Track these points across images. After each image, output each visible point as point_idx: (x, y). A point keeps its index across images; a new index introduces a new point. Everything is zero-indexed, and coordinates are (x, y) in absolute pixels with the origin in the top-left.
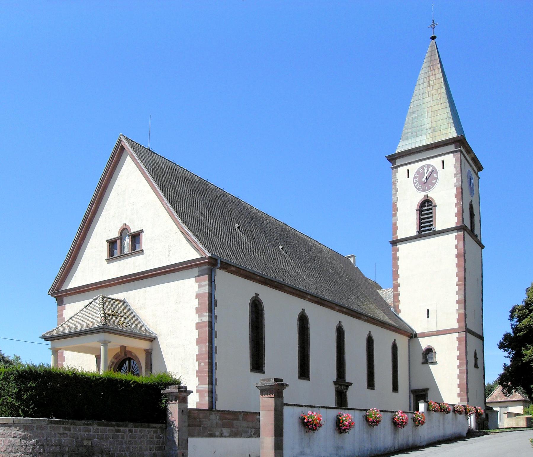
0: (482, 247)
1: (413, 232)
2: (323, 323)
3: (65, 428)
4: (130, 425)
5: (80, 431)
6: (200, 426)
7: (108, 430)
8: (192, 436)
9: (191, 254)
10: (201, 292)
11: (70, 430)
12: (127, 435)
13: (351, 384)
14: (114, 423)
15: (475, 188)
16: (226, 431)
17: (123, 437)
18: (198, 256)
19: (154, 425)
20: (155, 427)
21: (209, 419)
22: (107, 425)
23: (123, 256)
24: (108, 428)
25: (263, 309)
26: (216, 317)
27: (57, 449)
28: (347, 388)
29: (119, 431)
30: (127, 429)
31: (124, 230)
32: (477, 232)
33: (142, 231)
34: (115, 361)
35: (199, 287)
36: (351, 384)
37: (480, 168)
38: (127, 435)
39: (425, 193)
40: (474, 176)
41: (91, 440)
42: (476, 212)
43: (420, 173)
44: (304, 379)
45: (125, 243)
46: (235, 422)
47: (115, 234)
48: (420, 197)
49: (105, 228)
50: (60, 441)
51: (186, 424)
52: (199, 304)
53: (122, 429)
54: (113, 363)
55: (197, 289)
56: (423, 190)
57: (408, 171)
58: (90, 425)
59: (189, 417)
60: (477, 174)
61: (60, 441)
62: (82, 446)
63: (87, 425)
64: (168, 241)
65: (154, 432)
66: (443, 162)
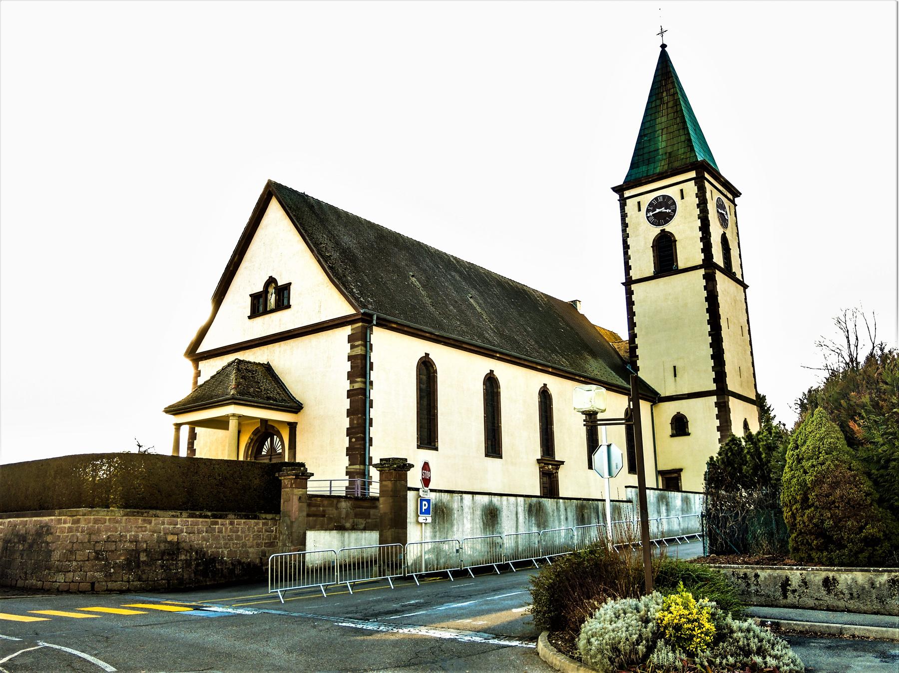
0: (745, 287)
1: (650, 270)
2: (520, 385)
3: (144, 521)
4: (231, 516)
5: (163, 523)
6: (324, 516)
7: (201, 524)
8: (312, 528)
9: (345, 309)
10: (354, 353)
11: (150, 523)
12: (226, 529)
13: (562, 463)
14: (209, 514)
15: (730, 218)
16: (362, 522)
17: (220, 531)
18: (353, 311)
19: (264, 516)
20: (266, 519)
21: (337, 508)
22: (200, 516)
23: (266, 312)
24: (201, 520)
25: (436, 372)
26: (371, 383)
27: (133, 547)
28: (558, 469)
29: (216, 523)
30: (228, 521)
31: (271, 281)
32: (735, 268)
33: (290, 284)
34: (255, 438)
35: (352, 347)
36: (562, 463)
37: (736, 194)
38: (226, 529)
39: (661, 228)
40: (727, 203)
41: (177, 534)
42: (733, 245)
43: (652, 206)
44: (493, 457)
45: (273, 297)
46: (372, 511)
47: (260, 288)
48: (656, 231)
49: (249, 280)
50: (136, 536)
51: (305, 514)
52: (352, 367)
53: (220, 521)
54: (252, 440)
55: (349, 350)
56: (659, 225)
57: (639, 203)
58: (177, 517)
59: (309, 505)
60: (733, 202)
61: (136, 536)
62: (166, 541)
63: (173, 516)
64: (317, 295)
65: (264, 524)
66: (682, 190)
